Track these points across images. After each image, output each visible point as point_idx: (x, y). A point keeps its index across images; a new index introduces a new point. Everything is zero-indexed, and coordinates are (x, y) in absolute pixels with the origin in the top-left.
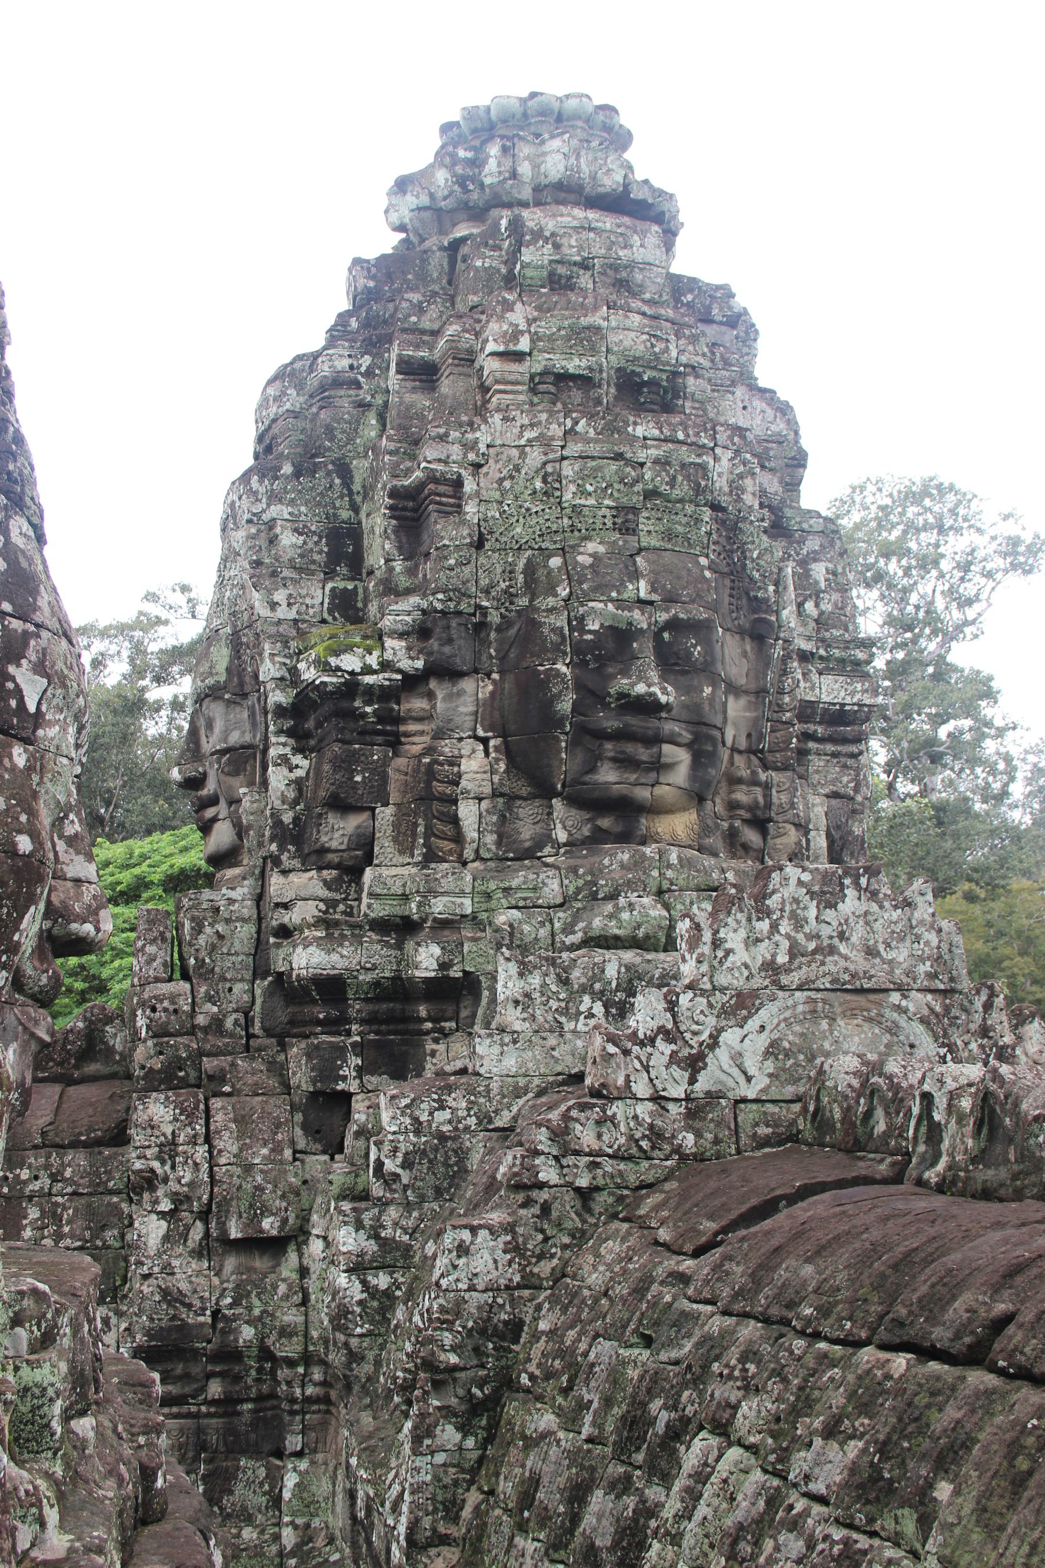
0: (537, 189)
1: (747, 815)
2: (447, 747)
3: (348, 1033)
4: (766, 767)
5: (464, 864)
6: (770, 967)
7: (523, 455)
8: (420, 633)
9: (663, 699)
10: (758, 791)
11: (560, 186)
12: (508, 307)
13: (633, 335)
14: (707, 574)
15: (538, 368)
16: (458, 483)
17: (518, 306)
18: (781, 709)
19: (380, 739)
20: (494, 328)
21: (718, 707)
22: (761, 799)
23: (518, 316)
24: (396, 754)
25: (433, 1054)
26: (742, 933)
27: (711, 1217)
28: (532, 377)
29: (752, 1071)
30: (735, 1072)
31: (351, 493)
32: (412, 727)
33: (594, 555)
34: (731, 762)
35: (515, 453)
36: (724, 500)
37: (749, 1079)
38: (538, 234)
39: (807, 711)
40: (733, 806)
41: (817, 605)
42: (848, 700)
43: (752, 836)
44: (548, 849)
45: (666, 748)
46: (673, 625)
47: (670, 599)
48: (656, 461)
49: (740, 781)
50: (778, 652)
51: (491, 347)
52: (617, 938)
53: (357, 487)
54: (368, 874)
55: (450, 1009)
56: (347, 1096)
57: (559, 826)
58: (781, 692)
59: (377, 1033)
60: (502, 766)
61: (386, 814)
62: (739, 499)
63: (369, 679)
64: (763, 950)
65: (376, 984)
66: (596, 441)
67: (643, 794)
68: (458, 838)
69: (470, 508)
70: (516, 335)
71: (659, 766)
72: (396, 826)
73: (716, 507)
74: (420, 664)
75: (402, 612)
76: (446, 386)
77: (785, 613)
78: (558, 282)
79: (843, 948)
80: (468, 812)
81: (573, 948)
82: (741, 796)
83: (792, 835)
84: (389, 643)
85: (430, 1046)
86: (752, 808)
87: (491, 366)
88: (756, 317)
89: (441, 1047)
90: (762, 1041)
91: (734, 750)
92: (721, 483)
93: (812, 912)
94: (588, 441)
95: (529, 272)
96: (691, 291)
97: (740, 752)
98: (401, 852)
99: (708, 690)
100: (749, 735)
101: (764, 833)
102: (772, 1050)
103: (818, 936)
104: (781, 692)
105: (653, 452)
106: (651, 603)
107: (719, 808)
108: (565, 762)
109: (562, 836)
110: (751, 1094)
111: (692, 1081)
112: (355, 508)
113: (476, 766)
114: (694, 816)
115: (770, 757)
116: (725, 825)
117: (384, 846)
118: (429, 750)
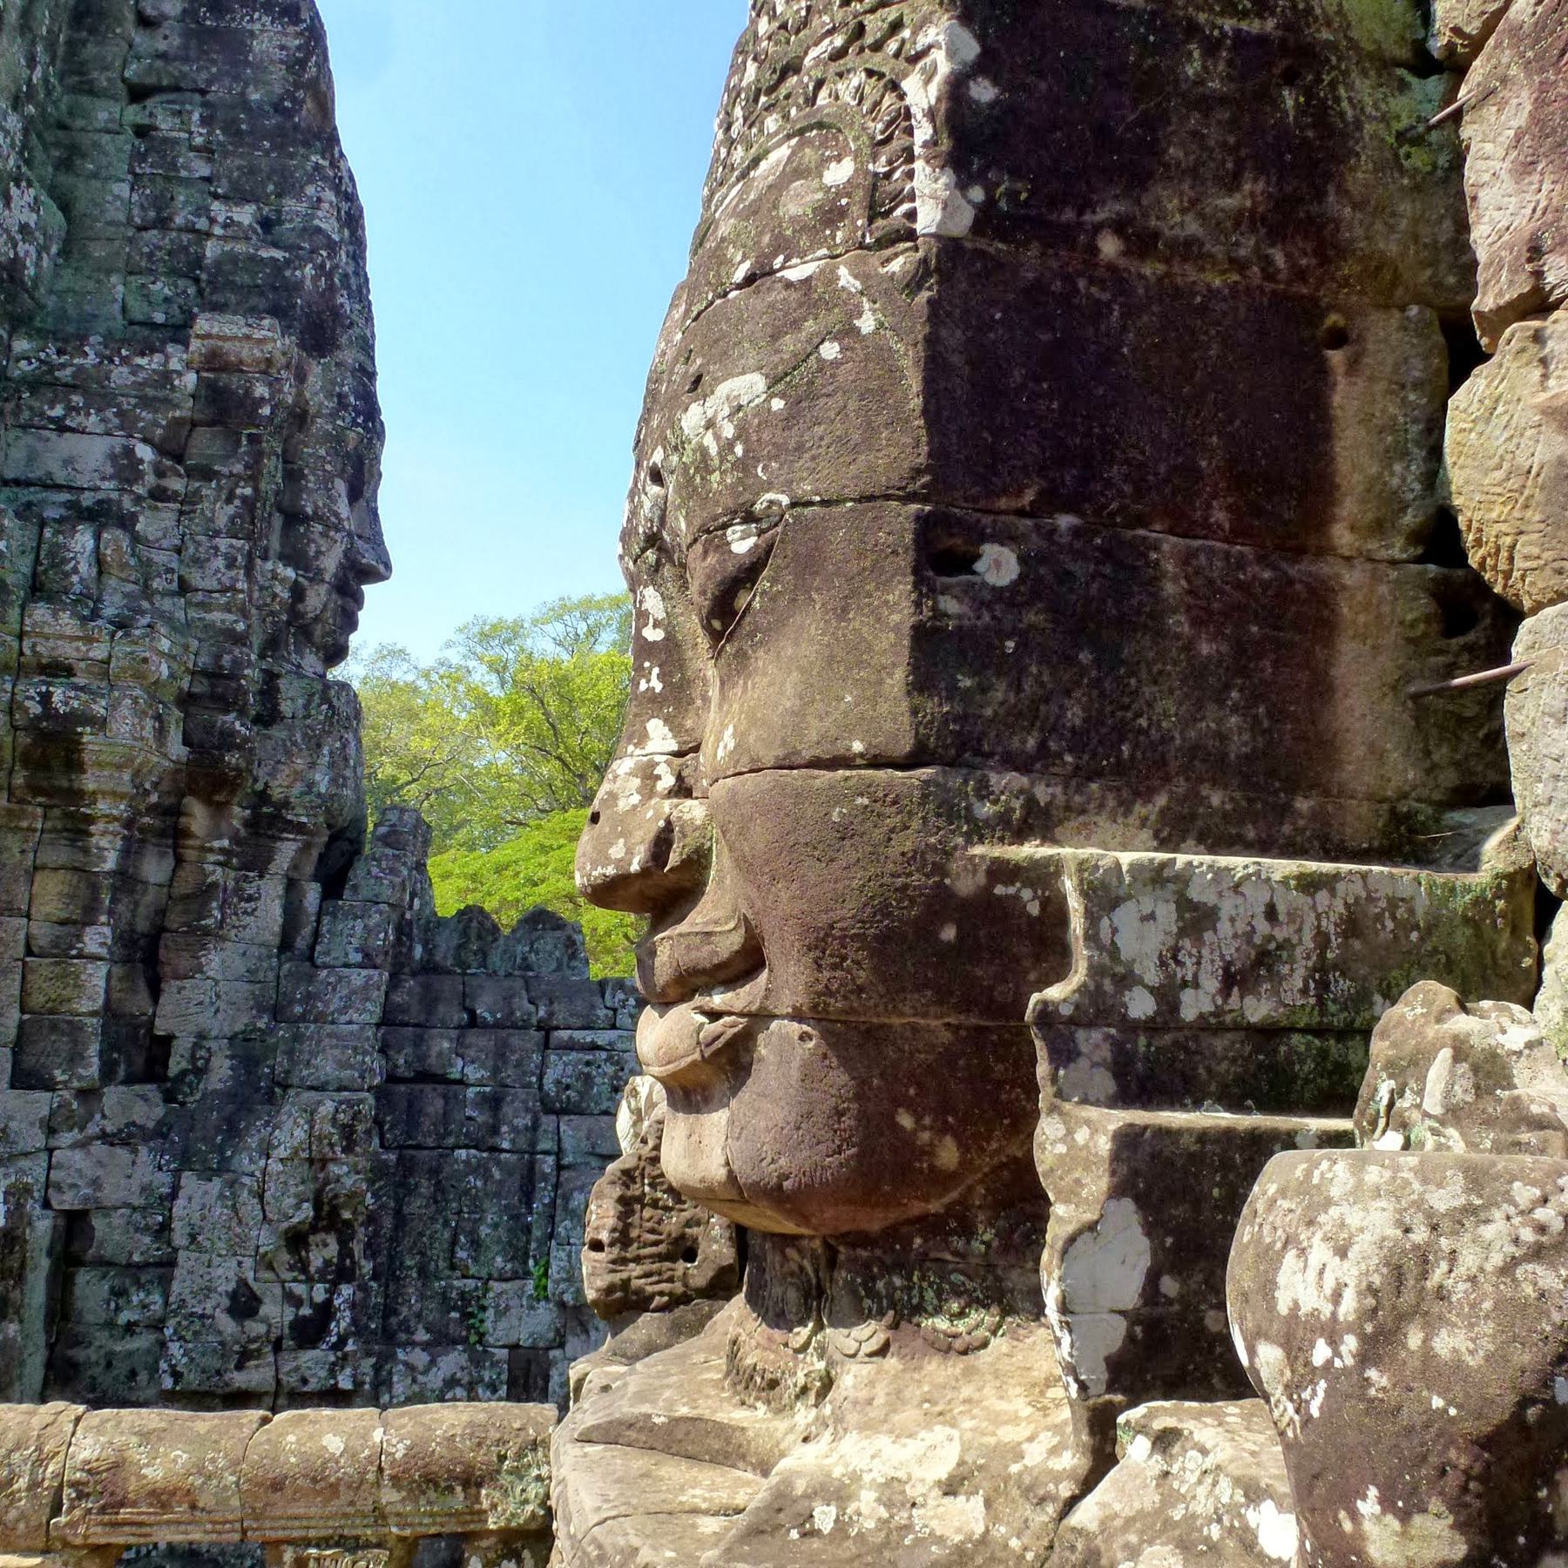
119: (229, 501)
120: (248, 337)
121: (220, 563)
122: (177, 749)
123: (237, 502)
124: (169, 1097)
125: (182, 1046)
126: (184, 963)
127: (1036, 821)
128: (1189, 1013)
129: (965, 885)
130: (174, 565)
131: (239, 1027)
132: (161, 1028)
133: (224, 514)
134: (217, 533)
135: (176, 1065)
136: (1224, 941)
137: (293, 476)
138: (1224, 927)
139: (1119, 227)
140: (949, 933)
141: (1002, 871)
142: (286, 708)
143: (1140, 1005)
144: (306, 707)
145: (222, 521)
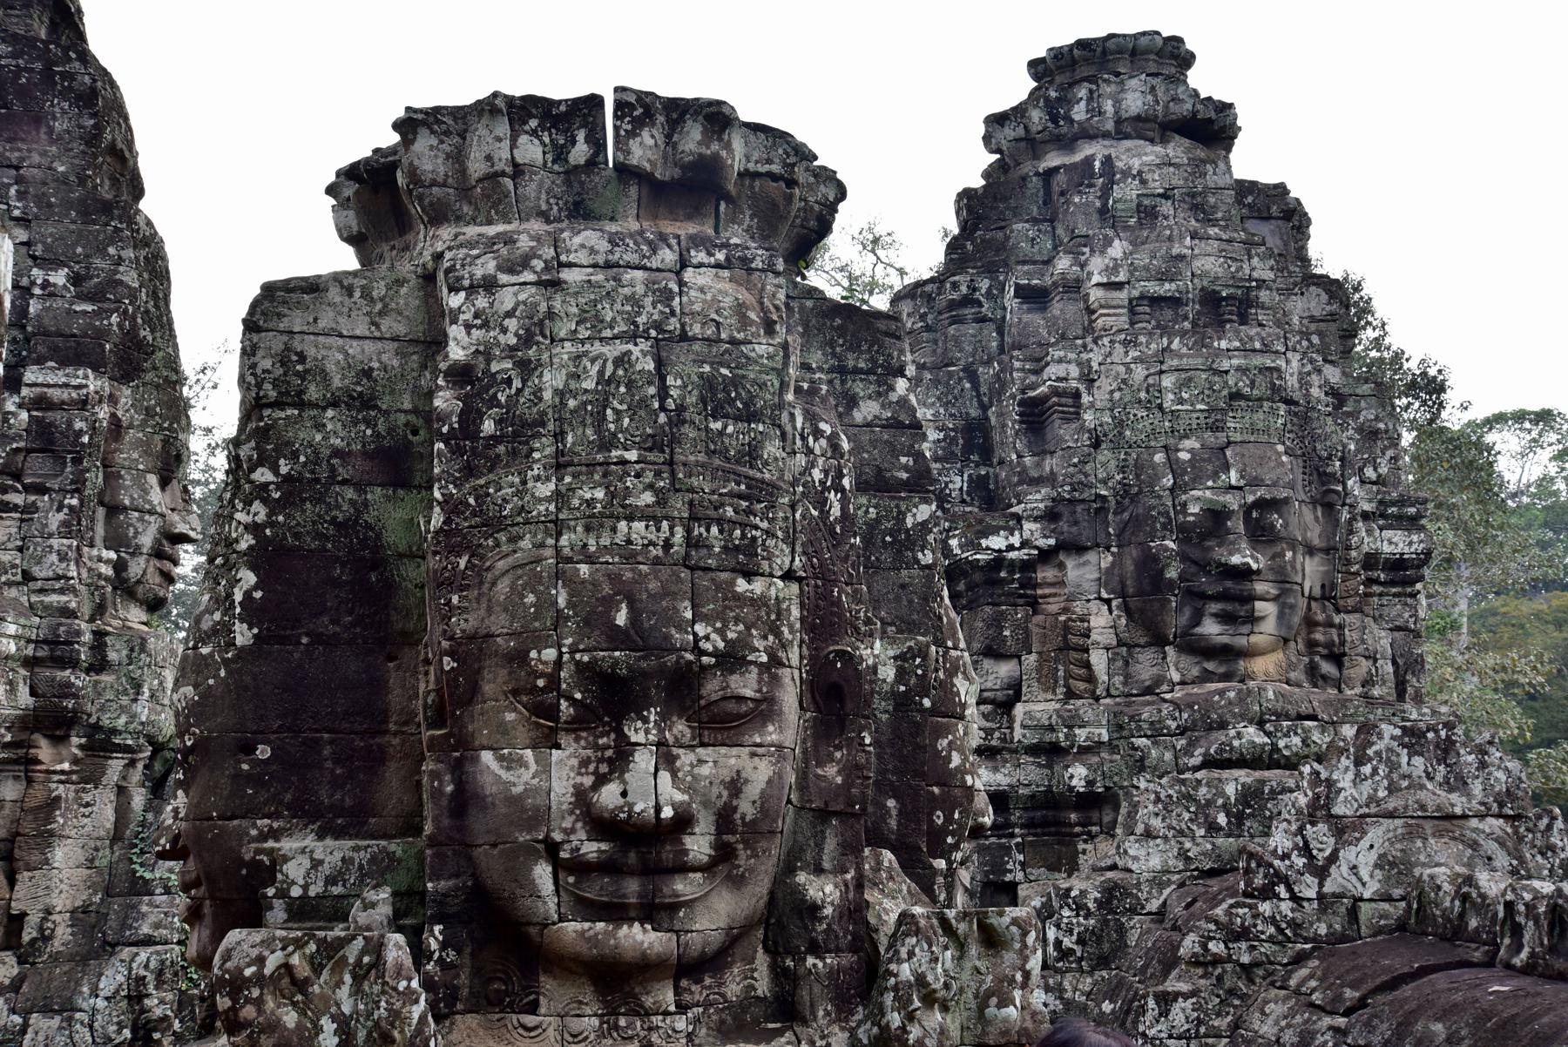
0: (1119, 122)
1: (1325, 652)
2: (1078, 607)
3: (1012, 836)
4: (1338, 611)
5: (1097, 699)
6: (1373, 799)
7: (1129, 371)
8: (1050, 516)
9: (1255, 566)
10: (1334, 633)
11: (1138, 119)
12: (1108, 242)
13: (1212, 259)
14: (1284, 458)
15: (1136, 293)
16: (1077, 395)
17: (1117, 243)
18: (1349, 562)
19: (1021, 601)
20: (1097, 264)
21: (1299, 567)
22: (1336, 638)
23: (1117, 249)
24: (1035, 612)
25: (1084, 852)
26: (1350, 775)
27: (1353, 987)
28: (1131, 301)
29: (1366, 878)
30: (1354, 879)
31: (978, 395)
32: (1047, 591)
33: (1190, 451)
34: (1309, 608)
35: (1122, 369)
36: (1297, 396)
37: (1364, 884)
38: (1126, 173)
39: (1371, 560)
40: (1311, 645)
41: (1375, 469)
42: (1406, 550)
43: (1327, 668)
44: (1165, 687)
45: (1259, 605)
46: (1261, 504)
47: (1255, 483)
48: (1239, 369)
49: (1317, 624)
50: (1345, 515)
51: (1096, 279)
52: (1229, 760)
53: (984, 389)
54: (1019, 710)
55: (1095, 816)
56: (1014, 886)
57: (1172, 668)
58: (1349, 548)
59: (1034, 835)
60: (1124, 621)
61: (1031, 660)
62: (1308, 394)
63: (1013, 555)
64: (1366, 788)
65: (1033, 796)
66: (1188, 356)
67: (1242, 641)
68: (1091, 678)
69: (1088, 417)
70: (1115, 269)
71: (1253, 619)
72: (1039, 670)
73: (1289, 402)
74: (1052, 542)
75: (1037, 499)
76: (1056, 308)
77: (1350, 483)
78: (1147, 214)
79: (1429, 786)
80: (1098, 660)
81: (1196, 769)
82: (1319, 636)
83: (1365, 664)
84: (1027, 526)
85: (1081, 846)
86: (1329, 645)
87: (1095, 295)
88: (1309, 207)
89: (1089, 847)
90: (1373, 856)
91: (1311, 598)
92: (1292, 381)
93: (1404, 759)
94: (1181, 357)
95: (1119, 206)
96: (1251, 193)
97: (1316, 599)
98: (1045, 691)
99: (1289, 555)
100: (1323, 586)
101: (1340, 666)
102: (1382, 863)
103: (1409, 776)
104: (1349, 548)
105: (1235, 362)
106: (1240, 488)
107: (1301, 646)
108: (1175, 619)
109: (1176, 677)
110: (1367, 895)
111: (1321, 885)
112: (984, 408)
113: (1102, 622)
114: (1281, 655)
115: (1341, 602)
116: (1306, 659)
117: (1030, 688)
118: (1065, 610)
119: (59, 510)
120: (66, 385)
121: (54, 557)
122: (24, 698)
123: (66, 510)
124: (21, 961)
125: (33, 919)
126: (35, 857)
127: (275, 834)
128: (312, 893)
129: (247, 857)
130: (18, 562)
131: (78, 903)
132: (16, 907)
133: (55, 520)
134: (51, 536)
135: (28, 934)
136: (326, 869)
137: (111, 476)
138: (326, 865)
139: (307, 635)
140: (244, 872)
141: (258, 851)
142: (112, 656)
143: (296, 892)
144: (129, 657)
145: (53, 526)
